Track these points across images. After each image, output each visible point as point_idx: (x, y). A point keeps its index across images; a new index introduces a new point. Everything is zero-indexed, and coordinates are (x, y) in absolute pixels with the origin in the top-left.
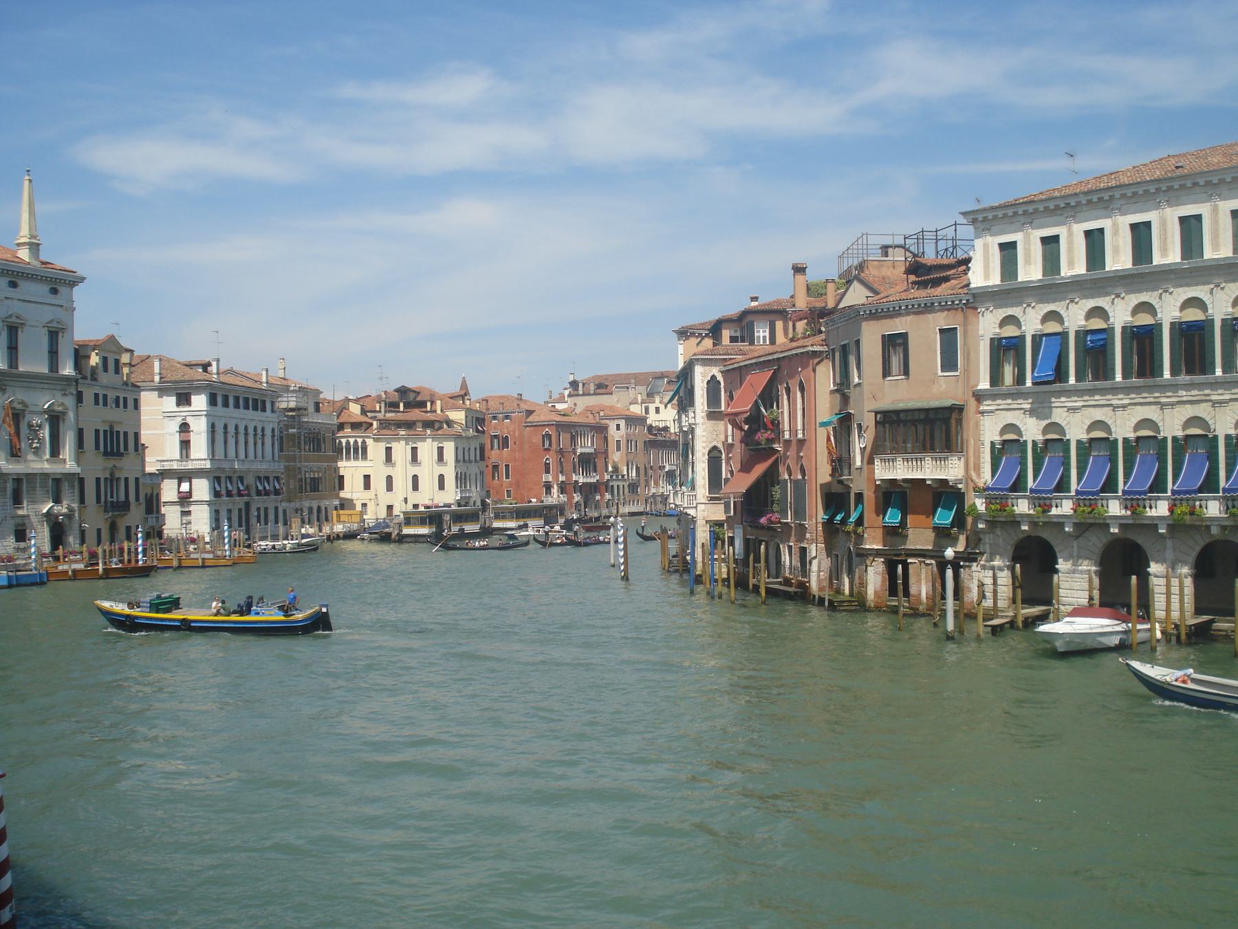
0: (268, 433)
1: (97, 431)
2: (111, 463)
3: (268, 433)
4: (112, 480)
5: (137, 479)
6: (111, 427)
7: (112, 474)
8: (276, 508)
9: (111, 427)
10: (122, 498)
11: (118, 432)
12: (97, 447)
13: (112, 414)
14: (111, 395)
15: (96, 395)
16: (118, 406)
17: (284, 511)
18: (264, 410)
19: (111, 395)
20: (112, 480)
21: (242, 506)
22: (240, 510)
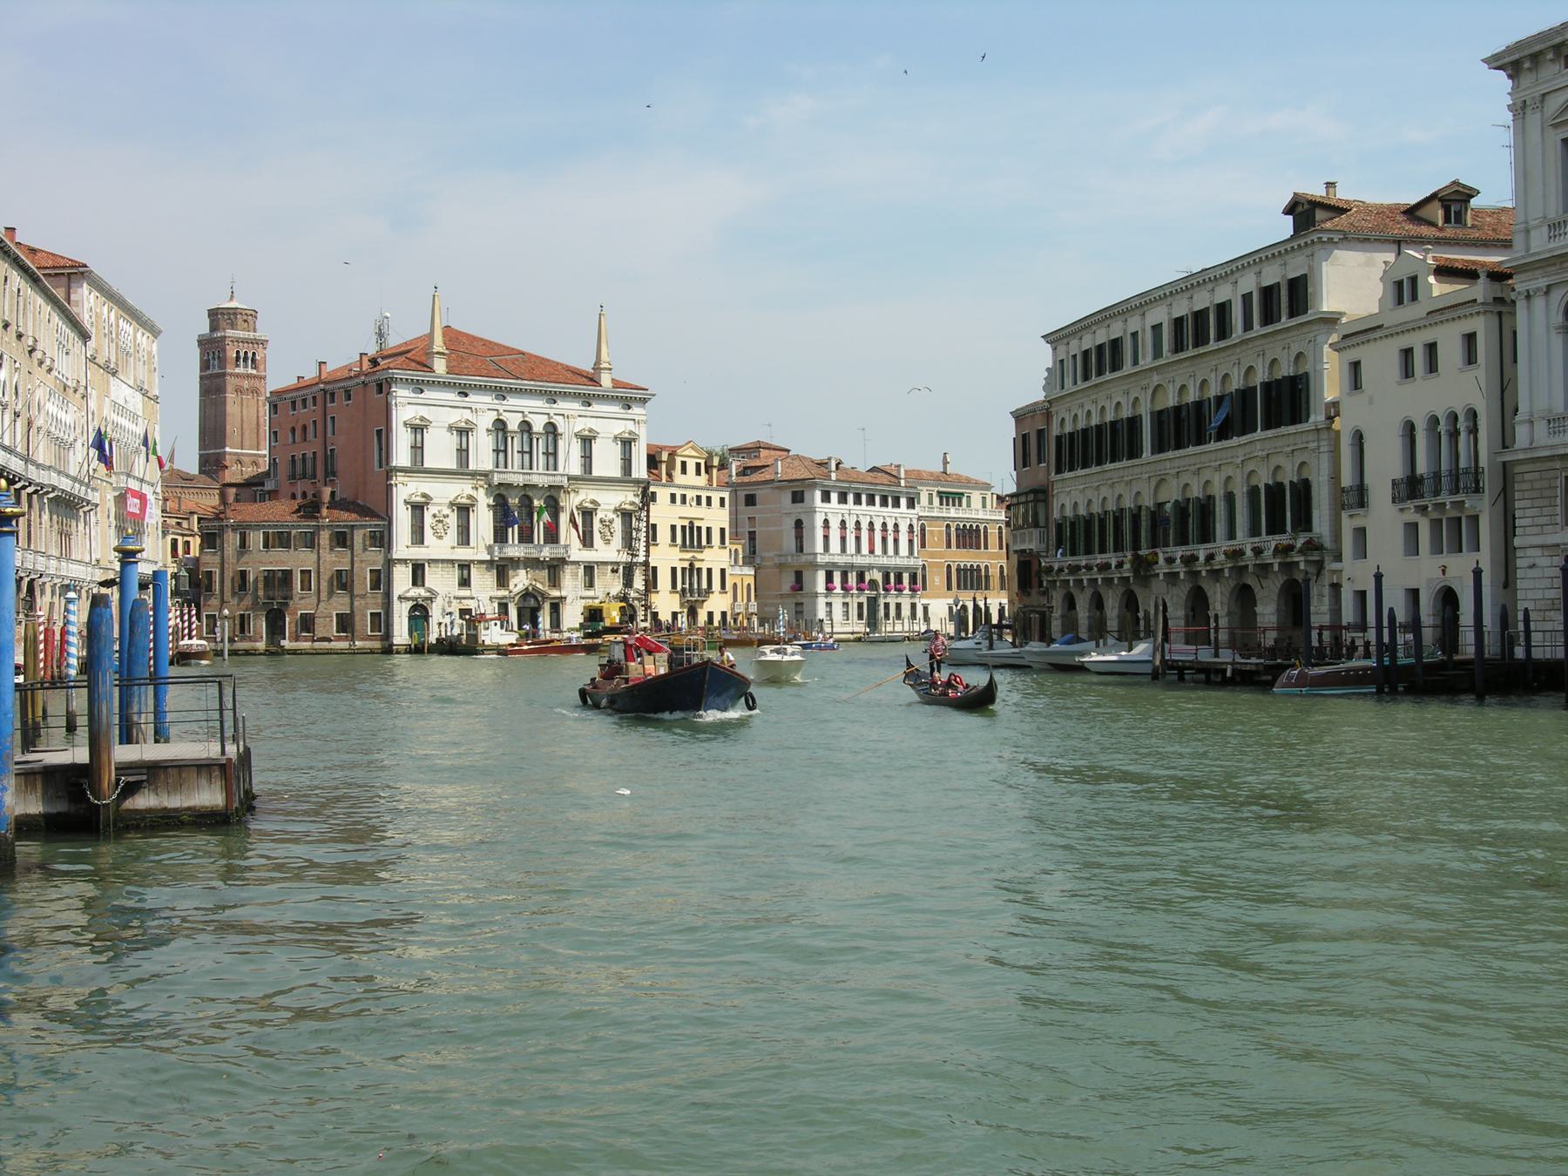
0: (903, 528)
1: (673, 528)
2: (688, 556)
3: (903, 528)
4: (692, 570)
5: (723, 571)
6: (691, 523)
7: (691, 565)
8: (913, 606)
9: (691, 523)
10: (704, 585)
11: (699, 529)
12: (674, 538)
13: (691, 511)
14: (691, 494)
15: (673, 496)
16: (699, 502)
17: (926, 609)
18: (897, 504)
19: (691, 494)
20: (692, 570)
21: (863, 599)
22: (860, 605)
